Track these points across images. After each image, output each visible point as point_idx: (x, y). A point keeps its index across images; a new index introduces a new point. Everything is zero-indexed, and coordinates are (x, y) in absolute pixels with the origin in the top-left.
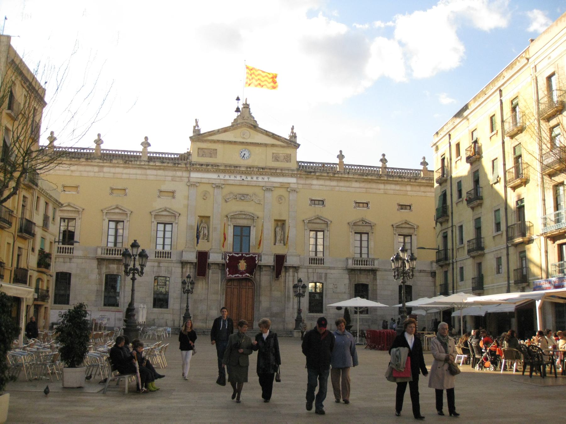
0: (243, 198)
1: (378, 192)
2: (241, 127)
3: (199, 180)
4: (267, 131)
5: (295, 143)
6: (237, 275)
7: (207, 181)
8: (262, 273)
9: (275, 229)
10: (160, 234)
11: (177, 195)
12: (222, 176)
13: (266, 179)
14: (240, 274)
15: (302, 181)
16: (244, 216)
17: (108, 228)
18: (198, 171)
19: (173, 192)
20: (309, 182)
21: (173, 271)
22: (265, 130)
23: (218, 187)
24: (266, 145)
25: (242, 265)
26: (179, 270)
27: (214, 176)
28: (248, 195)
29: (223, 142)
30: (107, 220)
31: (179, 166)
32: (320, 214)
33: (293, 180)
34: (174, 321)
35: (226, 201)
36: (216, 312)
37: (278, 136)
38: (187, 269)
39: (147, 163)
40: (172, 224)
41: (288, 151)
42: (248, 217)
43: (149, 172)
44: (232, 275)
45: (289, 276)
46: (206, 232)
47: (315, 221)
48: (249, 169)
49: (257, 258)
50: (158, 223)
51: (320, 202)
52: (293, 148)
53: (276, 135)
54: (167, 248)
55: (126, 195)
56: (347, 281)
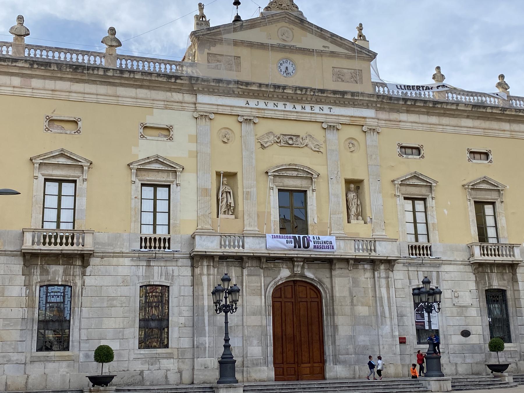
0: (290, 142)
1: (501, 134)
2: (278, 21)
3: (214, 109)
4: (322, 29)
5: (369, 51)
7: (227, 111)
8: (334, 273)
10: (148, 206)
11: (175, 133)
12: (253, 103)
13: (326, 110)
15: (383, 115)
16: (295, 173)
17: (44, 194)
18: (211, 92)
19: (168, 129)
20: (394, 116)
21: (176, 274)
22: (318, 28)
23: (248, 121)
24: (321, 53)
26: (187, 271)
27: (241, 102)
28: (298, 136)
29: (251, 45)
30: (42, 179)
31: (178, 81)
32: (419, 171)
33: (370, 113)
34: (180, 372)
35: (263, 147)
36: (260, 348)
37: (341, 38)
38: (202, 269)
39: (118, 74)
40: (169, 186)
41: (357, 64)
42: (301, 174)
43: (121, 91)
45: (379, 277)
46: (231, 200)
47: (411, 182)
48: (299, 92)
50: (143, 185)
51: (414, 151)
52: (364, 60)
53: (337, 36)
54: (162, 231)
55: (78, 131)
56: (472, 286)
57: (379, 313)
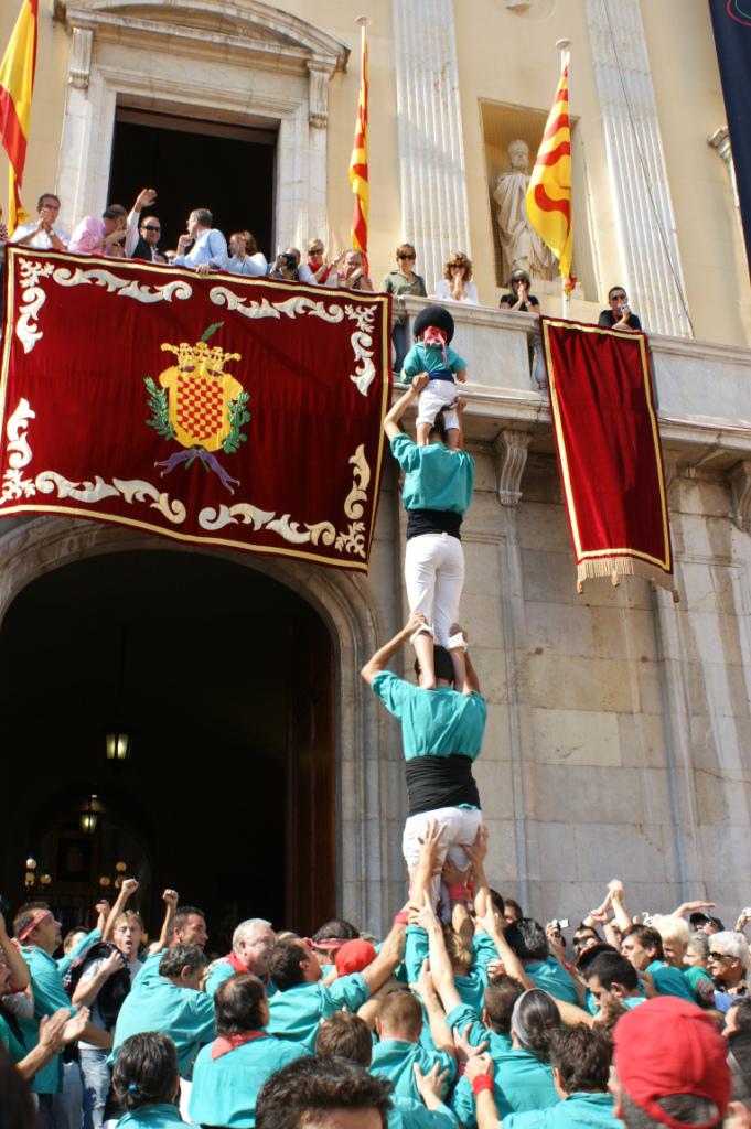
6: (135, 489)
9: (493, 188)
14: (175, 486)
25: (200, 396)
44: (79, 474)
49: (360, 342)
57: (683, 752)
